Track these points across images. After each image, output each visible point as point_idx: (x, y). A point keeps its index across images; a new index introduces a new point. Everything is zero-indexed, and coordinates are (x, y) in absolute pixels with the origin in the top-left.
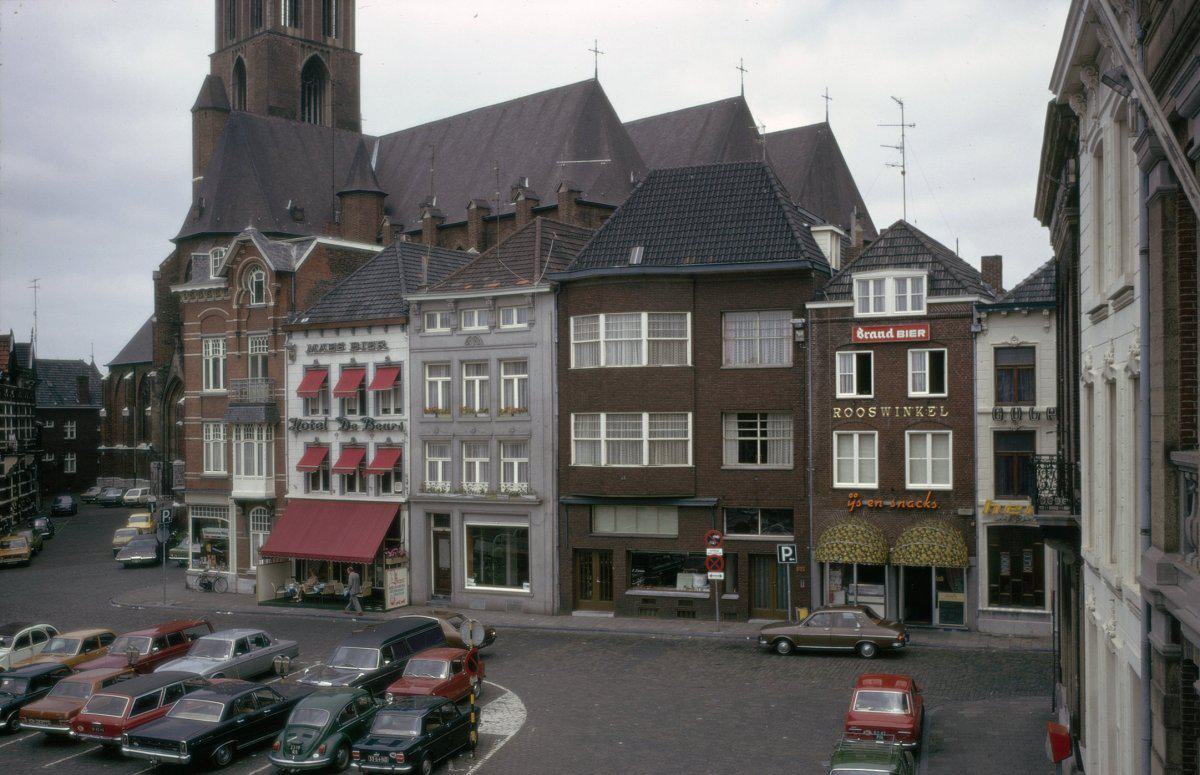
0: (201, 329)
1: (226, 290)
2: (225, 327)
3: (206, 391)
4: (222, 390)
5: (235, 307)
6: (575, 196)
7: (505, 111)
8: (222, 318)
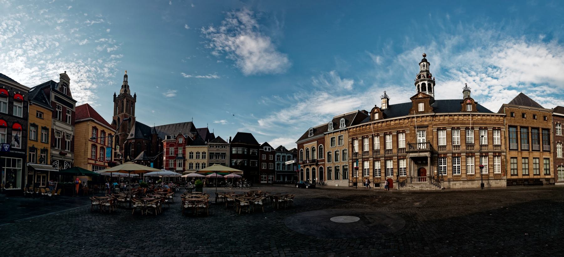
3: (169, 155)
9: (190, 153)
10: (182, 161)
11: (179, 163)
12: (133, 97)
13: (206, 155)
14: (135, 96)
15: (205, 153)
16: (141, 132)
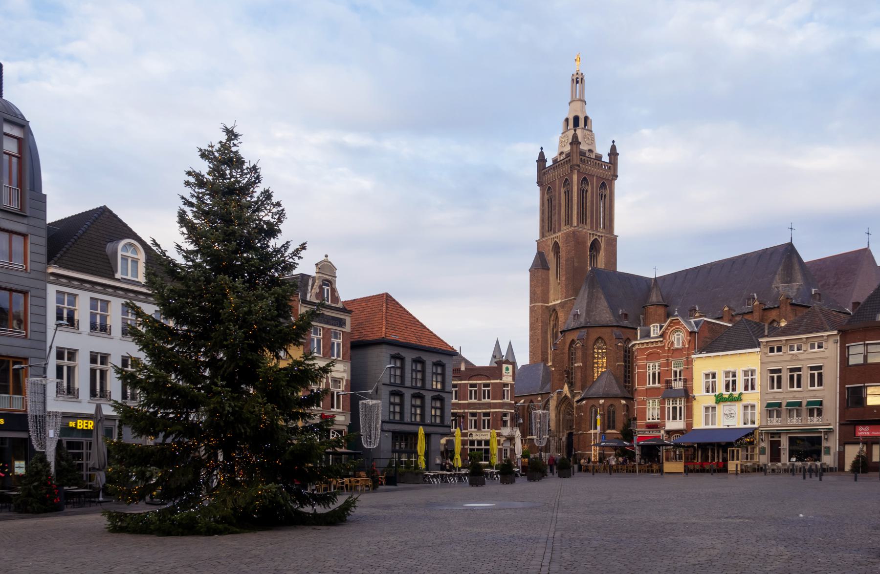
0: (647, 359)
1: (662, 341)
2: (660, 358)
3: (648, 385)
4: (657, 385)
5: (666, 348)
6: (789, 301)
7: (734, 262)
8: (658, 354)
9: (707, 375)
10: (681, 404)
11: (675, 409)
12: (606, 159)
13: (757, 377)
14: (613, 153)
15: (753, 372)
16: (605, 304)
